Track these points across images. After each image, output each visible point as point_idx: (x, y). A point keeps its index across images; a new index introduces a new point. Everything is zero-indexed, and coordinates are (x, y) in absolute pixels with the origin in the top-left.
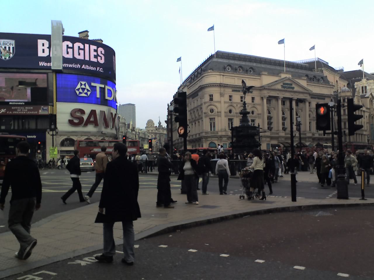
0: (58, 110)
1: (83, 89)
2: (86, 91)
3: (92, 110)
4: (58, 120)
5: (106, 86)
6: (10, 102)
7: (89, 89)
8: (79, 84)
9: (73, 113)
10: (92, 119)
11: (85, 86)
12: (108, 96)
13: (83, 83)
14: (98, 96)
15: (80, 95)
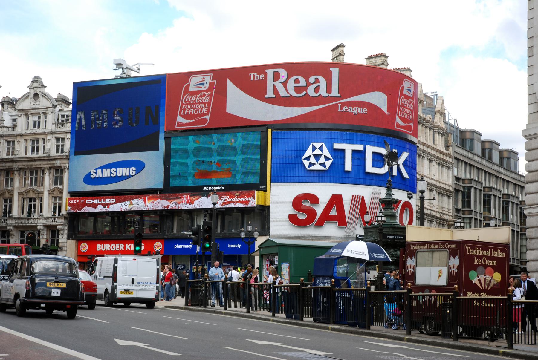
0: (273, 198)
1: (317, 157)
2: (322, 160)
3: (333, 195)
4: (272, 216)
5: (368, 147)
6: (205, 186)
7: (329, 156)
8: (310, 148)
9: (297, 202)
10: (333, 213)
11: (322, 151)
12: (373, 166)
13: (318, 145)
14: (348, 167)
15: (312, 168)
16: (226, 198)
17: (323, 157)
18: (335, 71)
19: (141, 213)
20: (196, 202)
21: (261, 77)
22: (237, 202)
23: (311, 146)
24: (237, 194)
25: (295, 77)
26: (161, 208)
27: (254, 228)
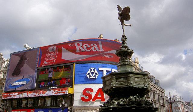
0: (75, 91)
1: (93, 73)
2: (94, 74)
5: (112, 70)
7: (97, 73)
13: (93, 69)
16: (57, 91)
17: (95, 74)
18: (100, 43)
19: (27, 99)
20: (46, 93)
21: (73, 45)
22: (60, 92)
23: (90, 69)
24: (61, 89)
25: (85, 44)
26: (33, 96)
27: (65, 103)
